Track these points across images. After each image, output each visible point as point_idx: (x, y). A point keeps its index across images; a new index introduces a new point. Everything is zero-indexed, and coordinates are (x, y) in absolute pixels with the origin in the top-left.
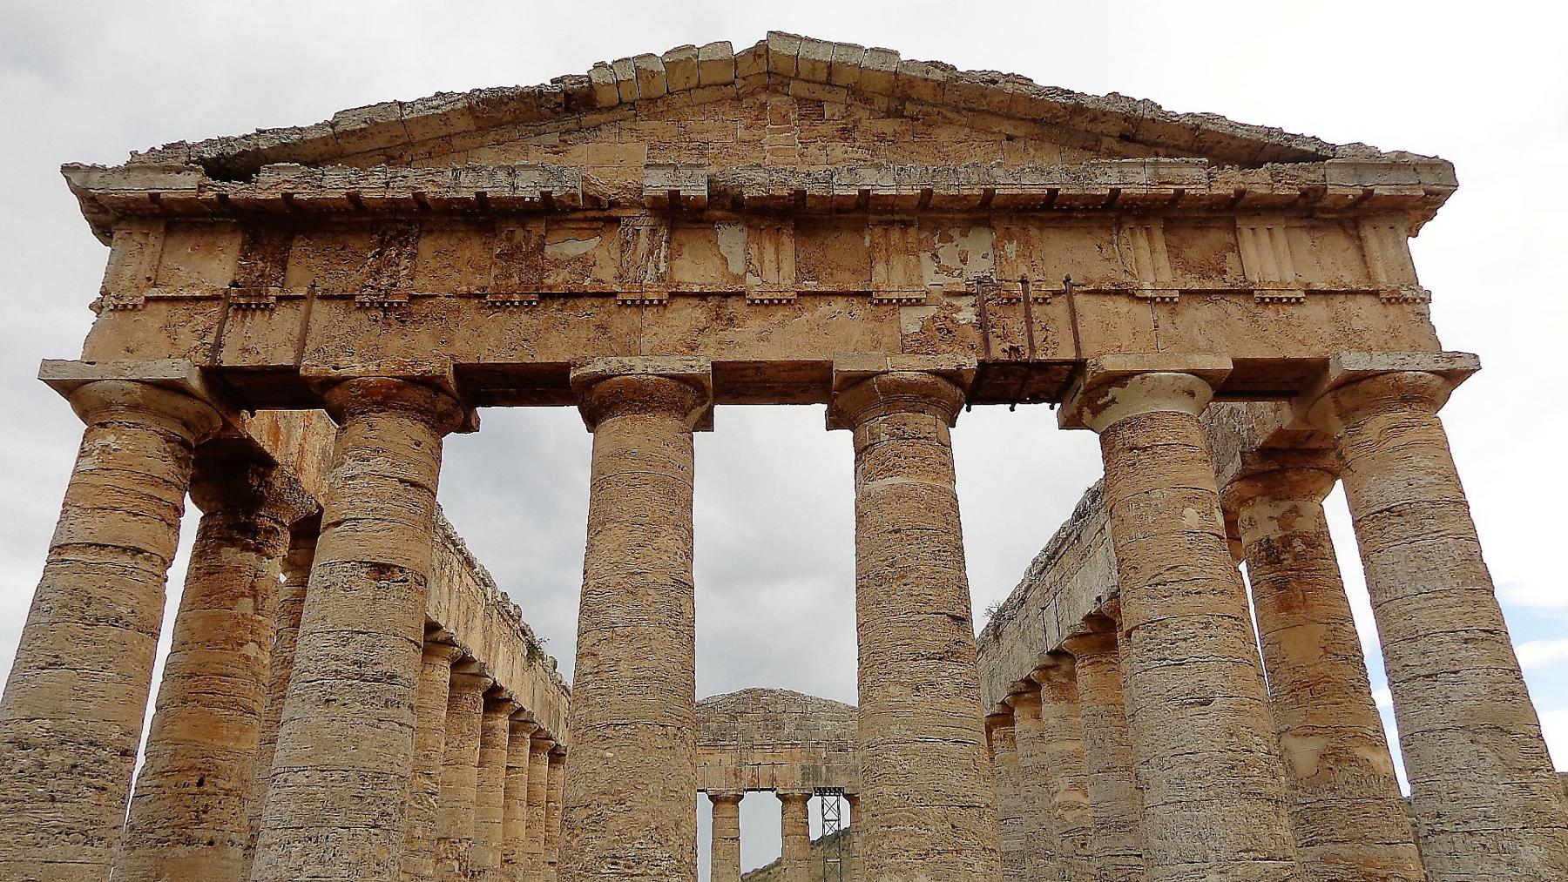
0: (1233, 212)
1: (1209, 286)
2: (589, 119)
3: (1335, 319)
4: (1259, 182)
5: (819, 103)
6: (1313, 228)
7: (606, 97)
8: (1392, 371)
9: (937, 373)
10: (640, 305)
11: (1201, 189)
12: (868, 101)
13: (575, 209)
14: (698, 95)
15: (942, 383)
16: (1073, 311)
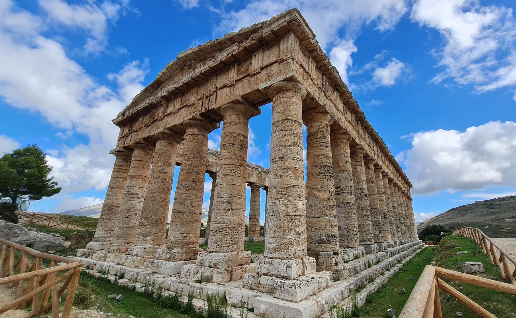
0: (248, 54)
1: (241, 77)
2: (163, 85)
3: (267, 74)
4: (247, 43)
5: (191, 65)
6: (270, 48)
7: (162, 79)
8: (271, 85)
9: (190, 119)
10: (161, 120)
11: (236, 52)
12: (197, 60)
13: (157, 104)
14: (176, 72)
15: (191, 121)
16: (216, 95)
